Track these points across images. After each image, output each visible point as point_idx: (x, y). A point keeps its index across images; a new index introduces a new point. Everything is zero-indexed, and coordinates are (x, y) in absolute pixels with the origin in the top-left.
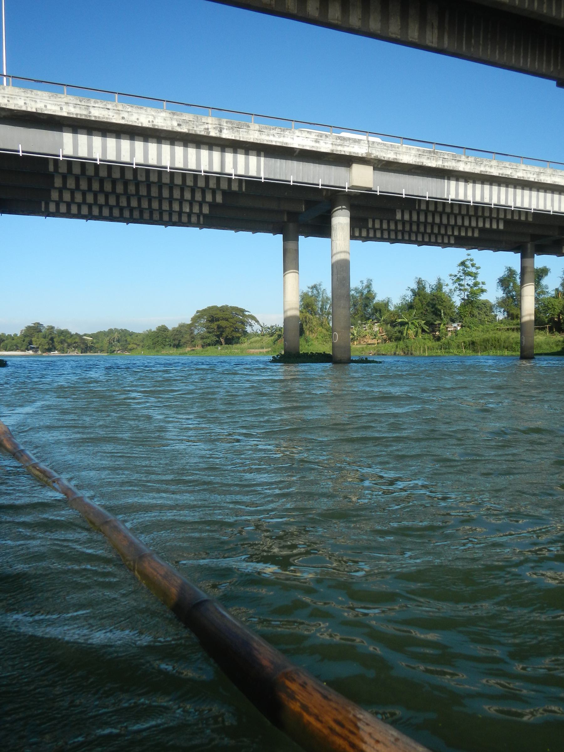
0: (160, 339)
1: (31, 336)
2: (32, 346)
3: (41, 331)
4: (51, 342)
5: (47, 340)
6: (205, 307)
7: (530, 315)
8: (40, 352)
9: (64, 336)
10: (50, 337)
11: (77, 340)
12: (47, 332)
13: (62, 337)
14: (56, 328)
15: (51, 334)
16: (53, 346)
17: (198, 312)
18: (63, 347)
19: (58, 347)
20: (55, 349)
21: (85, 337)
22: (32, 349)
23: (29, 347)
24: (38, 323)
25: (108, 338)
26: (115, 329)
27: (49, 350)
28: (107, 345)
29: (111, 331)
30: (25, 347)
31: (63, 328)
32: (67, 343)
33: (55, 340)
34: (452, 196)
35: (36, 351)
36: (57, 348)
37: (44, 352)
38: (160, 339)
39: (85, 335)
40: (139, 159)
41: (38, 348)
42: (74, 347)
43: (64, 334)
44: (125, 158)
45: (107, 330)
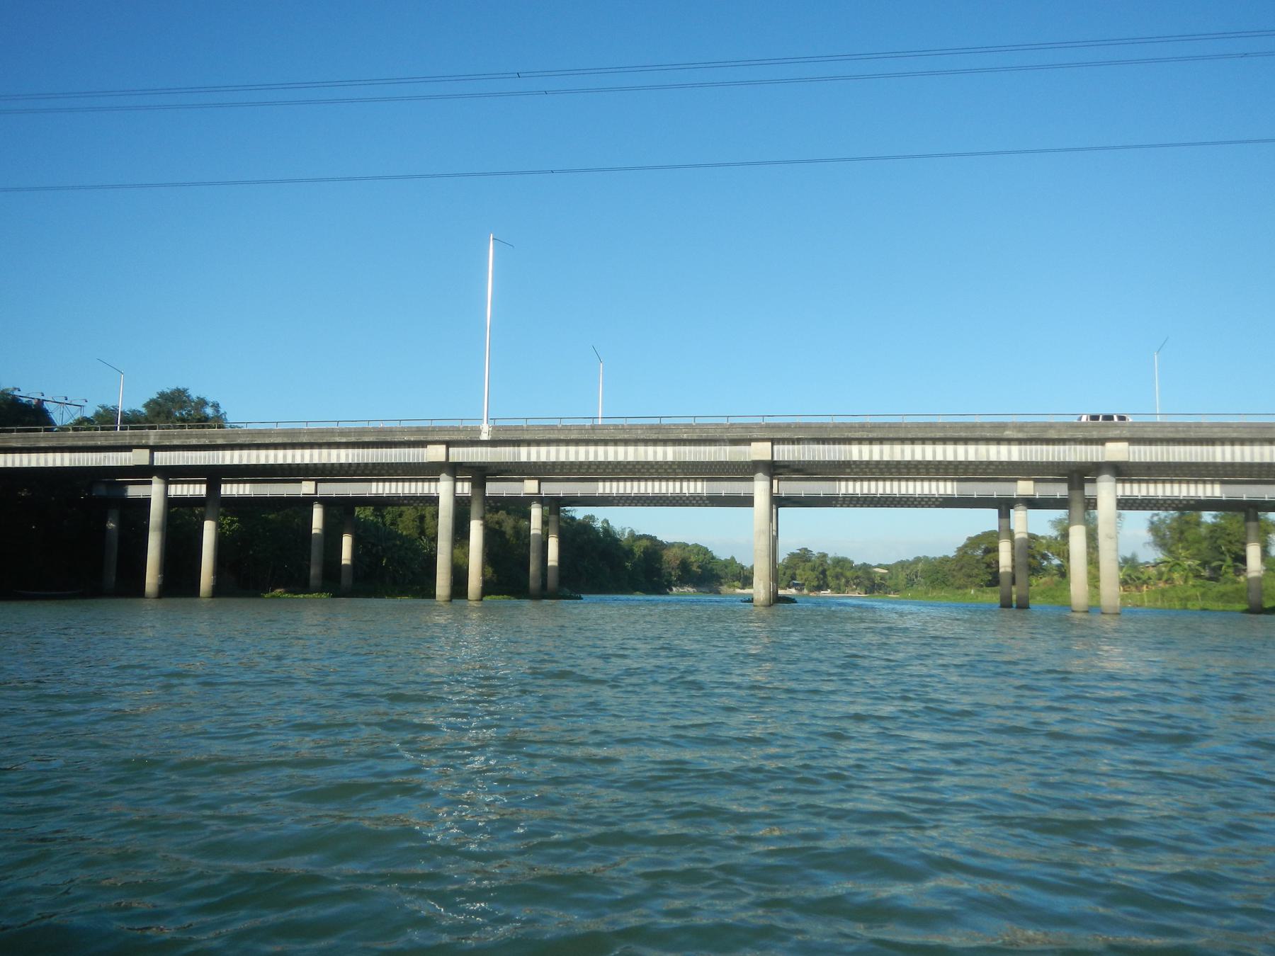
0: (939, 576)
1: (795, 567)
2: (795, 582)
3: (808, 560)
4: (821, 576)
5: (816, 573)
6: (979, 532)
7: (1005, 567)
8: (805, 591)
9: (842, 568)
10: (821, 568)
11: (860, 573)
12: (818, 562)
13: (838, 570)
14: (830, 556)
15: (822, 564)
16: (825, 582)
17: (969, 539)
18: (839, 585)
19: (832, 583)
20: (826, 586)
21: (877, 570)
22: (795, 586)
23: (791, 583)
24: (806, 549)
25: (908, 572)
26: (925, 556)
27: (819, 588)
28: (904, 583)
29: (918, 560)
30: (786, 583)
31: (840, 555)
32: (846, 577)
33: (828, 573)
34: (843, 491)
35: (801, 590)
36: (830, 585)
37: (811, 591)
38: (939, 576)
39: (880, 566)
40: (635, 491)
41: (803, 584)
42: (854, 584)
43: (841, 563)
44: (628, 491)
45: (911, 558)
